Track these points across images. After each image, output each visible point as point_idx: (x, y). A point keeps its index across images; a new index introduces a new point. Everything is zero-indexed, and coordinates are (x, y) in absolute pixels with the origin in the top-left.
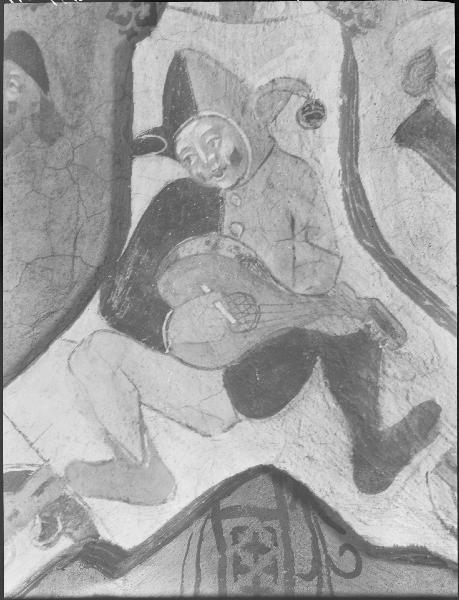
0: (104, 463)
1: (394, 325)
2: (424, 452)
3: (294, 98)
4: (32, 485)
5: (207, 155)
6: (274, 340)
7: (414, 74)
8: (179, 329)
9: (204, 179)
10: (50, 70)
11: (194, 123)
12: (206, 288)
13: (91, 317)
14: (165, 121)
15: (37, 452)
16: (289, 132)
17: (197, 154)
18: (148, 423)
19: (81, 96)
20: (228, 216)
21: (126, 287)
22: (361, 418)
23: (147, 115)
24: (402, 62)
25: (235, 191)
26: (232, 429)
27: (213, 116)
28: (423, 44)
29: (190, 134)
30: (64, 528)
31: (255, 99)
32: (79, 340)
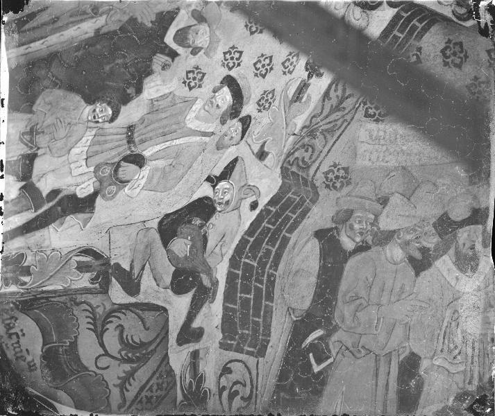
10: (247, 134)
12: (189, 238)
29: (223, 185)
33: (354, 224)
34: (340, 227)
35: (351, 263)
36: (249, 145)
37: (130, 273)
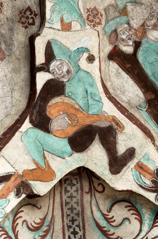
0: (34, 169)
1: (120, 124)
2: (131, 162)
3: (85, 53)
4: (13, 179)
5: (59, 71)
6: (83, 128)
7: (112, 37)
8: (55, 125)
9: (59, 79)
11: (55, 62)
12: (61, 113)
13: (27, 124)
14: (46, 61)
15: (14, 168)
16: (83, 63)
17: (56, 71)
18: (46, 156)
19: (11, 46)
20: (67, 90)
21: (37, 114)
22: (111, 152)
23: (40, 59)
24: (109, 34)
25: (68, 82)
26: (72, 156)
27: (61, 59)
28: (113, 29)
29: (53, 65)
30: (23, 191)
31: (73, 54)
32: (24, 131)
33: (122, 36)
34: (117, 43)
35: (140, 57)
36: (51, 28)
37: (38, 167)
